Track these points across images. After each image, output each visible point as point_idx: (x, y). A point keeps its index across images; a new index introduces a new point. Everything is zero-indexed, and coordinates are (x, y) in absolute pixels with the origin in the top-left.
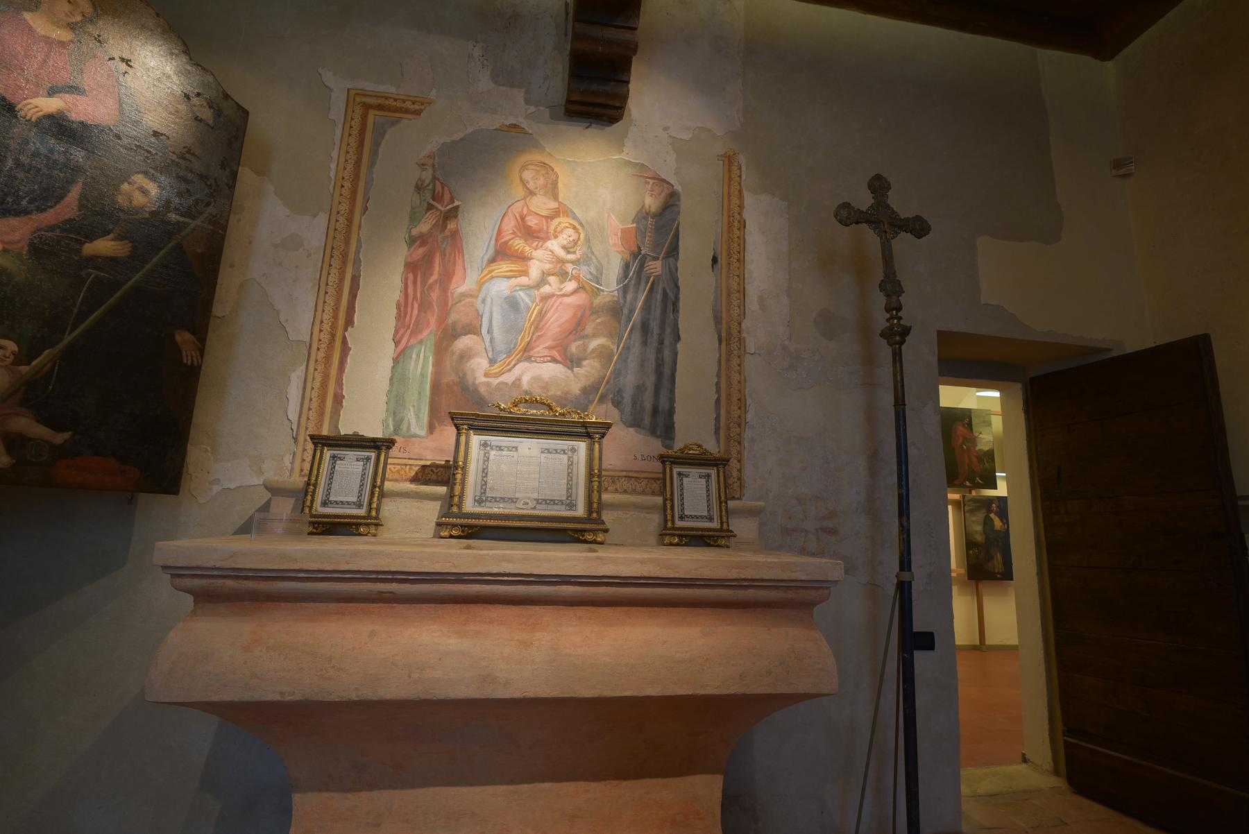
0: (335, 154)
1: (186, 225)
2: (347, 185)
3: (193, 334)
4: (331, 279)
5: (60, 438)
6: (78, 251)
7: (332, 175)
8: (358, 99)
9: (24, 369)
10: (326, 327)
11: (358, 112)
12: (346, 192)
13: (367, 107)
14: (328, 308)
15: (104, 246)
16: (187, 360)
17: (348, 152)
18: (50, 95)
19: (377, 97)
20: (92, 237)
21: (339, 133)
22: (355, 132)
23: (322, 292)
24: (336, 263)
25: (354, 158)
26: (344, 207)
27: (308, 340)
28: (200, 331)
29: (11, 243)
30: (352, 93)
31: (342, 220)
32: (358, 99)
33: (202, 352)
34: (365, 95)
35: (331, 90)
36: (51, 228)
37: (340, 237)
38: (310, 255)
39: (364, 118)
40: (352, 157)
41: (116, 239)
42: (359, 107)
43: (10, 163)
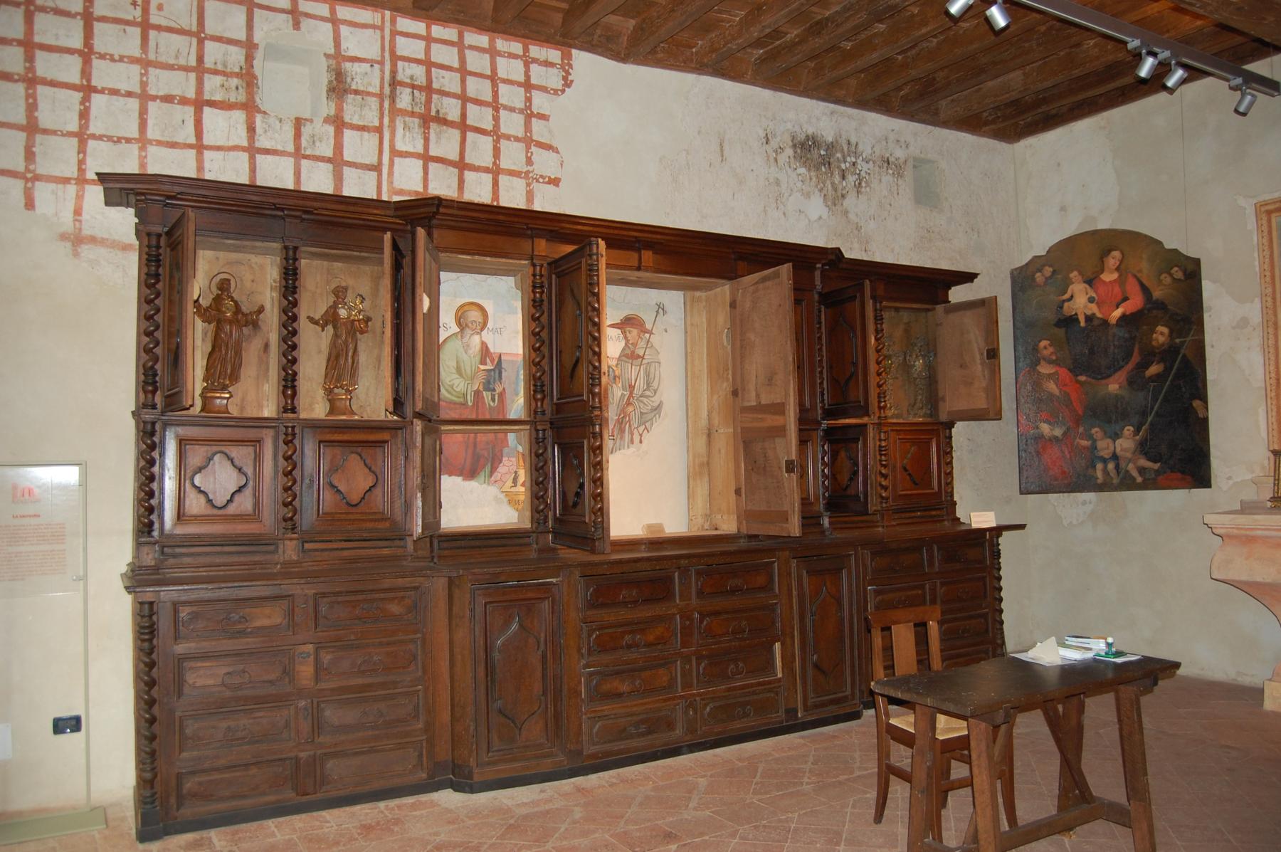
0: (1256, 255)
1: (1185, 341)
2: (1268, 274)
3: (1201, 400)
4: (1270, 342)
5: (1156, 466)
6: (1144, 377)
7: (1257, 269)
8: (1263, 209)
9: (1138, 437)
10: (1273, 375)
11: (1265, 218)
12: (1268, 279)
13: (1269, 213)
14: (1272, 362)
15: (1154, 369)
16: (1201, 416)
17: (1264, 250)
18: (1118, 308)
19: (1275, 203)
20: (1147, 369)
21: (1255, 238)
22: (1265, 233)
23: (1266, 353)
24: (1271, 330)
25: (1268, 253)
26: (1269, 290)
27: (1263, 386)
28: (1204, 399)
29: (1120, 383)
30: (1258, 205)
31: (1269, 299)
32: (1263, 209)
33: (1207, 408)
34: (1266, 205)
35: (1245, 209)
36: (1132, 370)
37: (1270, 312)
38: (1255, 329)
39: (1269, 221)
40: (1267, 253)
41: (1157, 364)
42: (1264, 215)
43: (1112, 347)
